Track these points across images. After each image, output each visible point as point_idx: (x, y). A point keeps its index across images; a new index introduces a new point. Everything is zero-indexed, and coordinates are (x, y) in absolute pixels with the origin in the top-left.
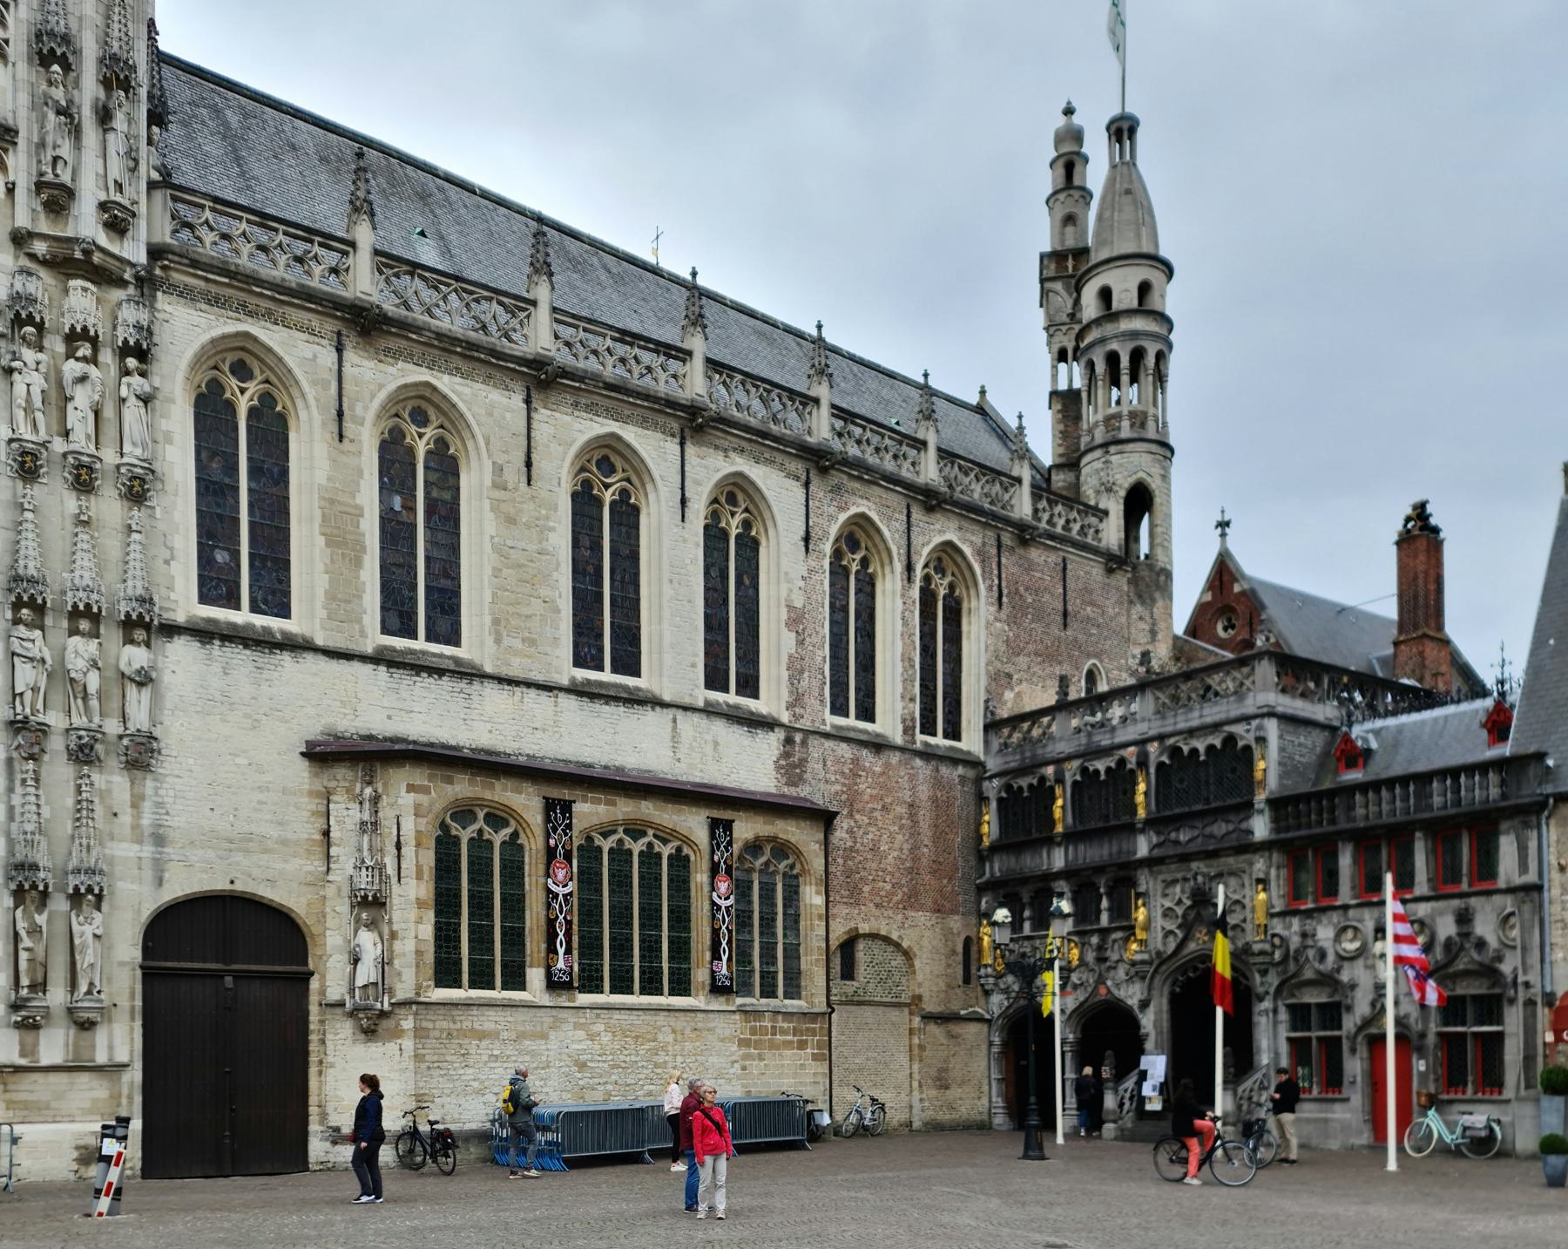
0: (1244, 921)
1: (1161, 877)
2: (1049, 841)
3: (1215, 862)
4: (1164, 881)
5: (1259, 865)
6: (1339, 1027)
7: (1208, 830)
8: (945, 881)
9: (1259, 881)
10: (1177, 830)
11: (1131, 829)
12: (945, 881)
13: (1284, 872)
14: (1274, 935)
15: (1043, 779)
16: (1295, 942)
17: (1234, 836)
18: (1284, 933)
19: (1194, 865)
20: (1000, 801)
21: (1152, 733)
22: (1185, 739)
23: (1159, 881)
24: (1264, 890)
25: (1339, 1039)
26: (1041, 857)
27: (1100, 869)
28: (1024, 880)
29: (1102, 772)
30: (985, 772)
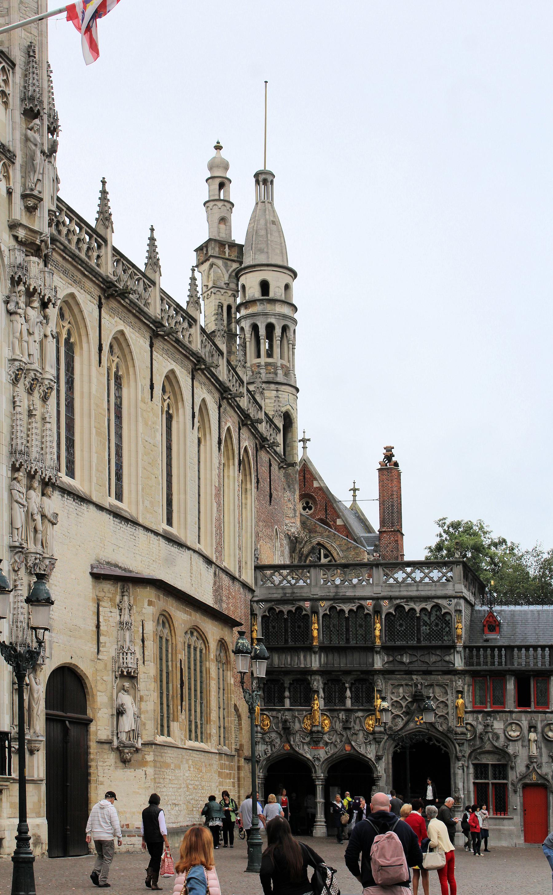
0: (447, 714)
1: (390, 682)
2: (309, 649)
4: (392, 685)
5: (459, 683)
6: (505, 777)
9: (461, 692)
11: (371, 649)
13: (471, 688)
14: (467, 724)
15: (300, 609)
16: (480, 728)
17: (440, 663)
18: (474, 723)
19: (414, 677)
20: (263, 617)
21: (383, 594)
22: (407, 602)
23: (389, 684)
24: (462, 698)
25: (506, 784)
26: (299, 659)
27: (347, 673)
28: (287, 672)
29: (347, 612)
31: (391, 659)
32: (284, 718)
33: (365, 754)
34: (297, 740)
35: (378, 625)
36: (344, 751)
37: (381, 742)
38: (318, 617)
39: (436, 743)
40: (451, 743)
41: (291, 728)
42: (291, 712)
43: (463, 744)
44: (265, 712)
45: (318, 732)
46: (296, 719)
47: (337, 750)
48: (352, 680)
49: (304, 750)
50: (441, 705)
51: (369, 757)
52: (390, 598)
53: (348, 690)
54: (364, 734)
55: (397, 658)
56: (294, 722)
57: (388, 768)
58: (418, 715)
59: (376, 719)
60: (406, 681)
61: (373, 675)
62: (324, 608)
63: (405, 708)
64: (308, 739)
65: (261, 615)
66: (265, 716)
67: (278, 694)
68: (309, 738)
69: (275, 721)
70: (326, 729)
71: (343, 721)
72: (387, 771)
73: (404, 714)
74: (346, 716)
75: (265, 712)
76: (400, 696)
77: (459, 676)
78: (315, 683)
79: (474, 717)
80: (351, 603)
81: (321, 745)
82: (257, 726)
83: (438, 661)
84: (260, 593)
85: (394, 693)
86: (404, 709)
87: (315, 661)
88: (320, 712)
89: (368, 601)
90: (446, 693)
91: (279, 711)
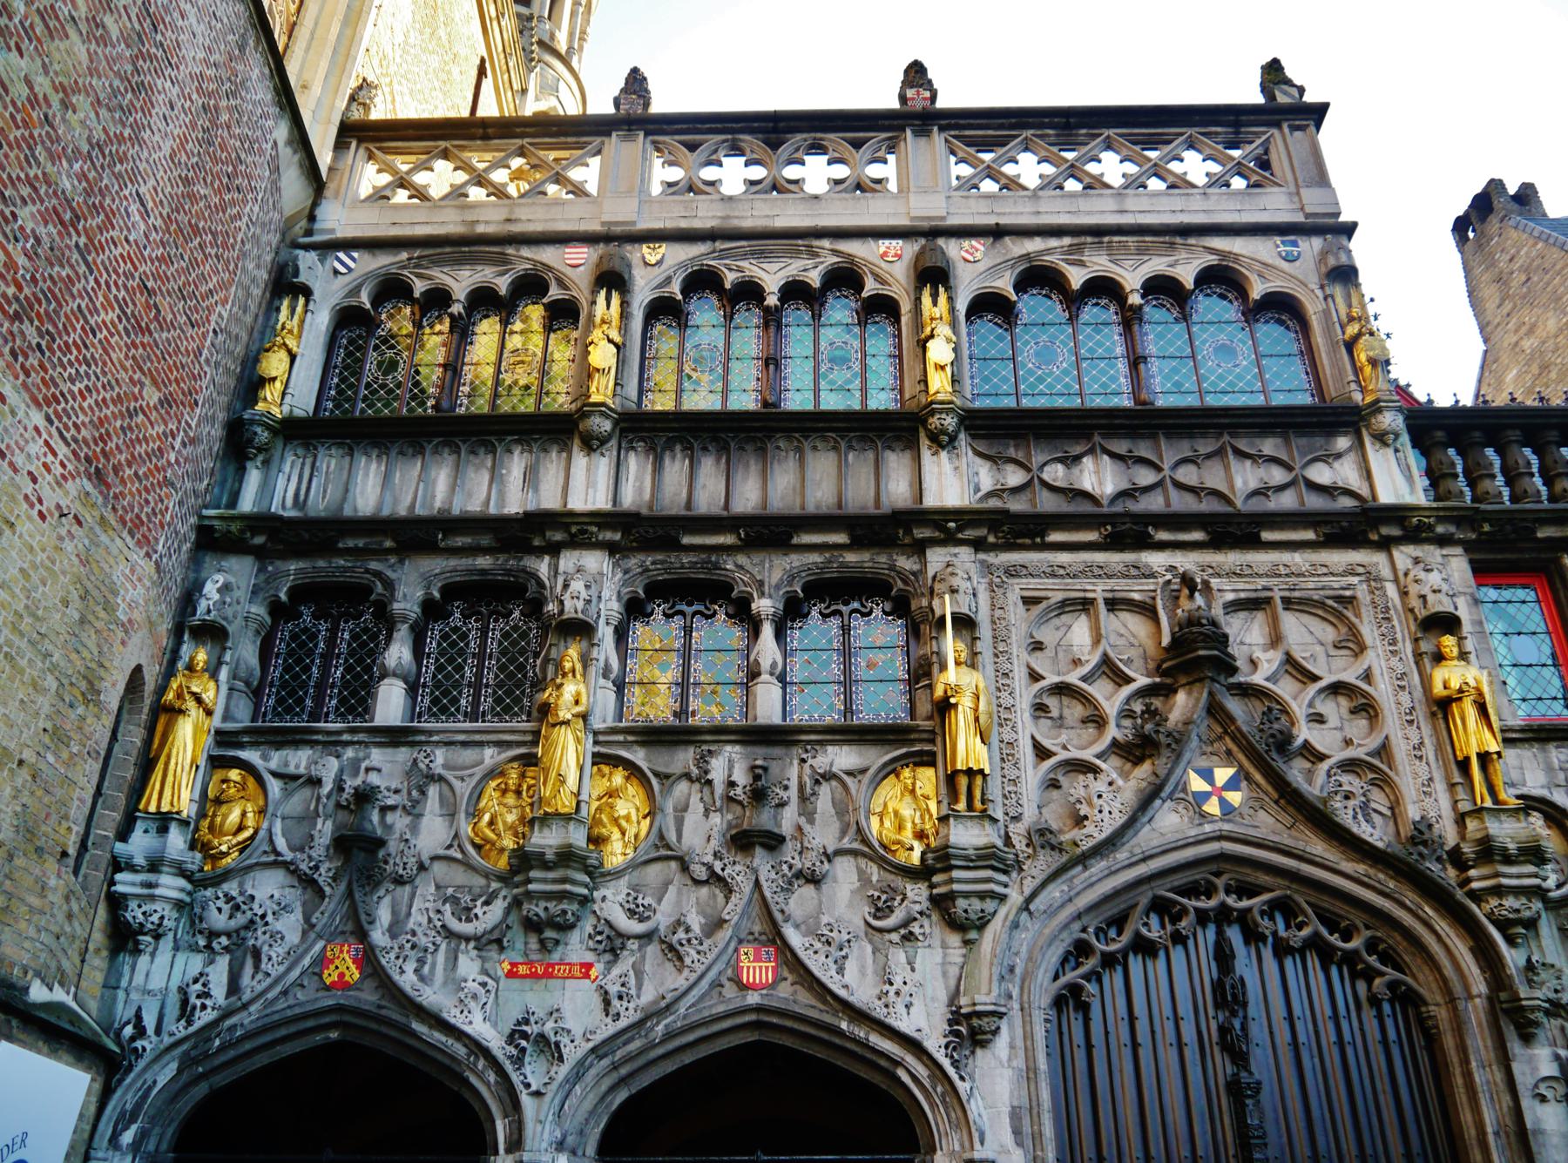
0: (1384, 751)
1: (1016, 589)
3: (1231, 559)
4: (1029, 602)
7: (1188, 475)
8: (152, 396)
10: (1071, 461)
12: (152, 396)
22: (1077, 249)
30: (309, 233)
31: (1015, 477)
32: (351, 783)
33: (879, 1012)
34: (417, 919)
35: (944, 330)
36: (730, 991)
37: (982, 924)
38: (625, 304)
39: (1324, 932)
40: (1442, 926)
41: (393, 846)
42: (403, 755)
43: (1531, 924)
44: (245, 755)
45: (567, 856)
46: (433, 791)
47: (681, 982)
48: (792, 578)
49: (456, 984)
50: (1335, 710)
51: (905, 1025)
52: (997, 233)
53: (767, 631)
55: (1045, 476)
56: (413, 811)
57: (1034, 1109)
58: (1203, 763)
59: (951, 779)
60: (1111, 583)
61: (919, 548)
62: (658, 275)
63: (1118, 726)
64: (490, 916)
65: (334, 301)
66: (234, 774)
67: (349, 669)
68: (498, 907)
69: (299, 801)
70: (616, 854)
71: (730, 799)
72: (1027, 1128)
73: (1115, 761)
74: (753, 768)
75: (245, 755)
76: (1077, 662)
77: (1411, 550)
78: (577, 586)
79: (1549, 769)
80: (795, 253)
81: (576, 948)
82: (163, 821)
83: (1281, 488)
84: (336, 219)
85: (1037, 646)
86: (1112, 732)
87: (590, 483)
89: (883, 245)
90: (1354, 644)
91: (332, 744)
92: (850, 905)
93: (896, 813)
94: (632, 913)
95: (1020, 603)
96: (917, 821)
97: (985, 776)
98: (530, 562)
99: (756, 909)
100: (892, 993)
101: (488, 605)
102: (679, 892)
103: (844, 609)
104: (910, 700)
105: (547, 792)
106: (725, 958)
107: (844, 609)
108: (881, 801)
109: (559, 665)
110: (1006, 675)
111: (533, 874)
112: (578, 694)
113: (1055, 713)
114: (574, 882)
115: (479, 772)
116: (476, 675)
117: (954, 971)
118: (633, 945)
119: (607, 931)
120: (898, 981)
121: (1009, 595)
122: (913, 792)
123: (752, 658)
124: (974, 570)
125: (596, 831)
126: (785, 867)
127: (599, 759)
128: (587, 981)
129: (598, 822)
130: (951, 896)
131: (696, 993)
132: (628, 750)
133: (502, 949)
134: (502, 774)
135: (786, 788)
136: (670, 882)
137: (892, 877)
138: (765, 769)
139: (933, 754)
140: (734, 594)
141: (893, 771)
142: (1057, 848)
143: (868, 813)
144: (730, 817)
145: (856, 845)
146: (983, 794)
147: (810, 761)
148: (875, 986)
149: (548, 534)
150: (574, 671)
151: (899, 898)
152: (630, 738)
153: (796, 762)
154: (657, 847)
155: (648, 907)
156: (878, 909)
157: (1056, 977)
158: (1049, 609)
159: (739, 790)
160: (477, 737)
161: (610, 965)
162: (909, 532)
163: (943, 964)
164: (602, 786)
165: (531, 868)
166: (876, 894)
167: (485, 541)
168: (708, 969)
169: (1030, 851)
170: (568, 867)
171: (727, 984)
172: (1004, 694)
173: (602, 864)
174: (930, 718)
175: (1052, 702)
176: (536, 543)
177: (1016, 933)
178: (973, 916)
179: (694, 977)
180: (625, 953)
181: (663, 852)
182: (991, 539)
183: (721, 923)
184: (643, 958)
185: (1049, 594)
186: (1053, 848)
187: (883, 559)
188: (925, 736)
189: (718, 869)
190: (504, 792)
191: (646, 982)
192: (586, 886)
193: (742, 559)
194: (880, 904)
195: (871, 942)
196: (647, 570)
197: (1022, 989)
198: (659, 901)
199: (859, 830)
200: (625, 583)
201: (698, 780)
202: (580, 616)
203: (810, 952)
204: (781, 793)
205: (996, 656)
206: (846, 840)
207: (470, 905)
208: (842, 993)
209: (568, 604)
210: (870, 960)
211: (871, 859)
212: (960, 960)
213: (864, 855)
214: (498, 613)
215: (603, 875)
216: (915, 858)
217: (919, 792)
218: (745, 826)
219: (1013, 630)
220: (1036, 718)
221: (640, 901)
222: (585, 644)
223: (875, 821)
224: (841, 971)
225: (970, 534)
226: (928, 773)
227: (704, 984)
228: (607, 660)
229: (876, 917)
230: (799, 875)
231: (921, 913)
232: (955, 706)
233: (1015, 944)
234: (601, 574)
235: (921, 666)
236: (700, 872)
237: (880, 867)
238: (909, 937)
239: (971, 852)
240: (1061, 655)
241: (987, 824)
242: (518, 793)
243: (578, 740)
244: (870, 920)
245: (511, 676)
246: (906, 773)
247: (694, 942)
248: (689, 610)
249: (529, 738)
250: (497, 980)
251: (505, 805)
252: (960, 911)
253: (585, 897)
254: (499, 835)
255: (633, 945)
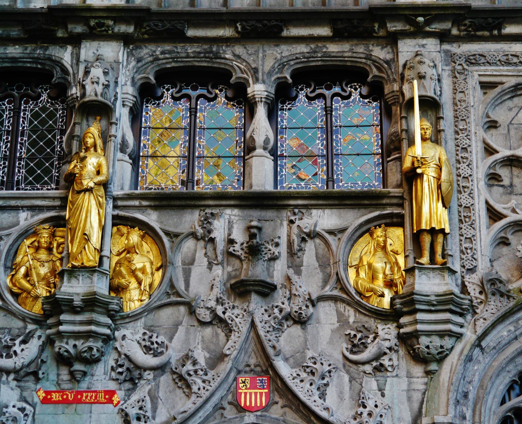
4: (486, 86)
47: (189, 405)
48: (282, 66)
53: (261, 112)
54: (342, 320)
68: (34, 345)
71: (230, 254)
74: (249, 228)
78: (97, 72)
85: (492, 125)
88: (110, 211)
92: (331, 342)
93: (370, 266)
94: (147, 349)
95: (478, 87)
96: (388, 272)
97: (445, 235)
98: (55, 52)
99: (252, 346)
100: (365, 415)
101: (19, 88)
102: (187, 332)
103: (327, 93)
104: (383, 171)
105: (74, 249)
106: (226, 386)
107: (327, 93)
108: (358, 256)
109: (82, 141)
110: (465, 149)
111: (63, 317)
112: (99, 166)
113: (506, 182)
114: (98, 324)
115: (15, 232)
116: (10, 150)
117: (417, 396)
118: (149, 375)
119: (127, 364)
120: (370, 404)
121: (469, 80)
122: (384, 248)
123: (248, 135)
124: (439, 58)
125: (116, 281)
126: (276, 311)
127: (117, 221)
128: (111, 406)
129: (119, 274)
130: (416, 335)
131: (202, 414)
132: (143, 213)
133: (38, 380)
134: (35, 233)
135: (277, 245)
136: (180, 323)
137: (366, 319)
138: (260, 229)
139: (401, 216)
140: (233, 80)
141: (368, 231)
142: (506, 295)
143: (347, 266)
144: (230, 269)
145: (336, 293)
146: (444, 250)
147: (297, 223)
148: (351, 409)
149: (70, 26)
150: (95, 146)
151: (371, 336)
152: (145, 203)
153: (285, 223)
154: (168, 294)
155: (161, 344)
156: (354, 346)
157: (503, 402)
158: (503, 93)
159: (237, 247)
160: (13, 203)
161: (129, 392)
162: (383, 25)
163: (408, 390)
164: (121, 243)
165: (62, 312)
166: (353, 333)
167: (14, 32)
168: (212, 395)
169: (483, 297)
170: (93, 311)
171: (228, 407)
172: (463, 166)
173: (122, 309)
174: (399, 186)
175: (504, 172)
176: (60, 34)
177: (470, 365)
178: (434, 351)
179: (200, 401)
180: (142, 382)
181: (174, 299)
182: (455, 32)
183: (222, 357)
184: (158, 386)
185: (504, 79)
186: (502, 295)
187: (361, 49)
188: (395, 201)
189: (220, 313)
190: (38, 249)
191: (160, 406)
192: (109, 327)
193: (239, 50)
194: (356, 342)
195: (348, 372)
196: (157, 59)
197: (474, 411)
198: (171, 339)
199: (339, 280)
200: (138, 71)
201: (203, 238)
202: (100, 98)
203: (297, 381)
204: (273, 249)
205: (457, 133)
206: (328, 288)
207: (10, 343)
208: (324, 414)
209: (89, 88)
210: (347, 388)
211: (349, 304)
212: (422, 387)
213: (343, 301)
214: (29, 96)
215: (123, 318)
216: (386, 303)
217: (389, 248)
218: (243, 277)
219: (472, 110)
220: (490, 186)
221: (154, 339)
222: (104, 123)
223: (352, 273)
224: (323, 396)
225: (436, 27)
226: (399, 231)
227: (209, 407)
228: (123, 137)
229: (352, 352)
230: (288, 317)
231: (390, 349)
232: (421, 175)
233: (469, 374)
234: (117, 62)
235: (392, 141)
236: (205, 315)
237: (356, 310)
238: (380, 369)
239: (433, 298)
240: (512, 132)
241: (446, 275)
242: (49, 250)
243: (100, 205)
244: (348, 354)
245: (41, 150)
246: (379, 232)
247: (200, 372)
248: (194, 94)
249: (57, 203)
250: (34, 406)
251: (38, 260)
252: (422, 347)
253: (108, 336)
254: (33, 285)
255: (149, 375)
